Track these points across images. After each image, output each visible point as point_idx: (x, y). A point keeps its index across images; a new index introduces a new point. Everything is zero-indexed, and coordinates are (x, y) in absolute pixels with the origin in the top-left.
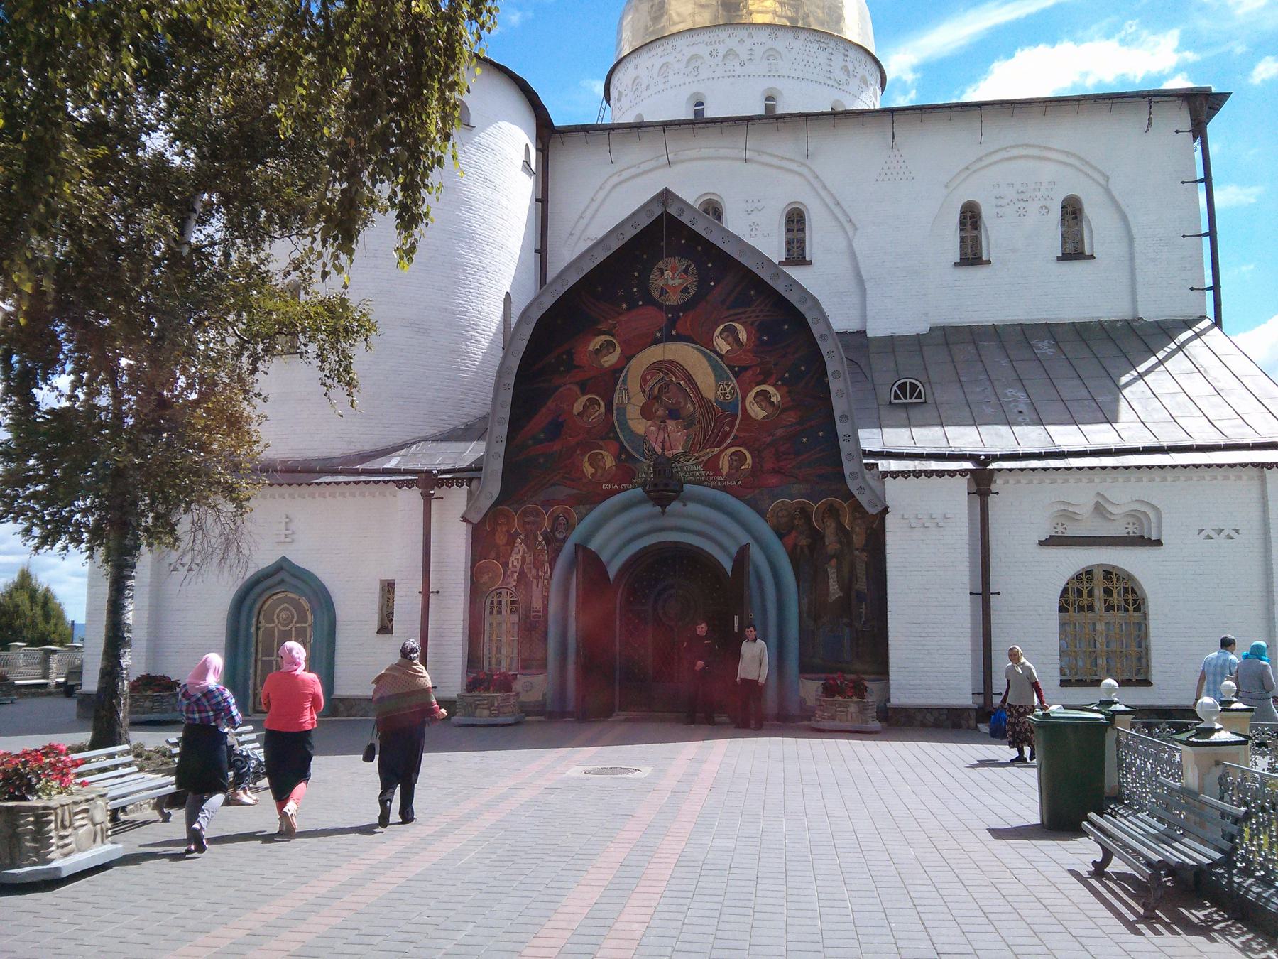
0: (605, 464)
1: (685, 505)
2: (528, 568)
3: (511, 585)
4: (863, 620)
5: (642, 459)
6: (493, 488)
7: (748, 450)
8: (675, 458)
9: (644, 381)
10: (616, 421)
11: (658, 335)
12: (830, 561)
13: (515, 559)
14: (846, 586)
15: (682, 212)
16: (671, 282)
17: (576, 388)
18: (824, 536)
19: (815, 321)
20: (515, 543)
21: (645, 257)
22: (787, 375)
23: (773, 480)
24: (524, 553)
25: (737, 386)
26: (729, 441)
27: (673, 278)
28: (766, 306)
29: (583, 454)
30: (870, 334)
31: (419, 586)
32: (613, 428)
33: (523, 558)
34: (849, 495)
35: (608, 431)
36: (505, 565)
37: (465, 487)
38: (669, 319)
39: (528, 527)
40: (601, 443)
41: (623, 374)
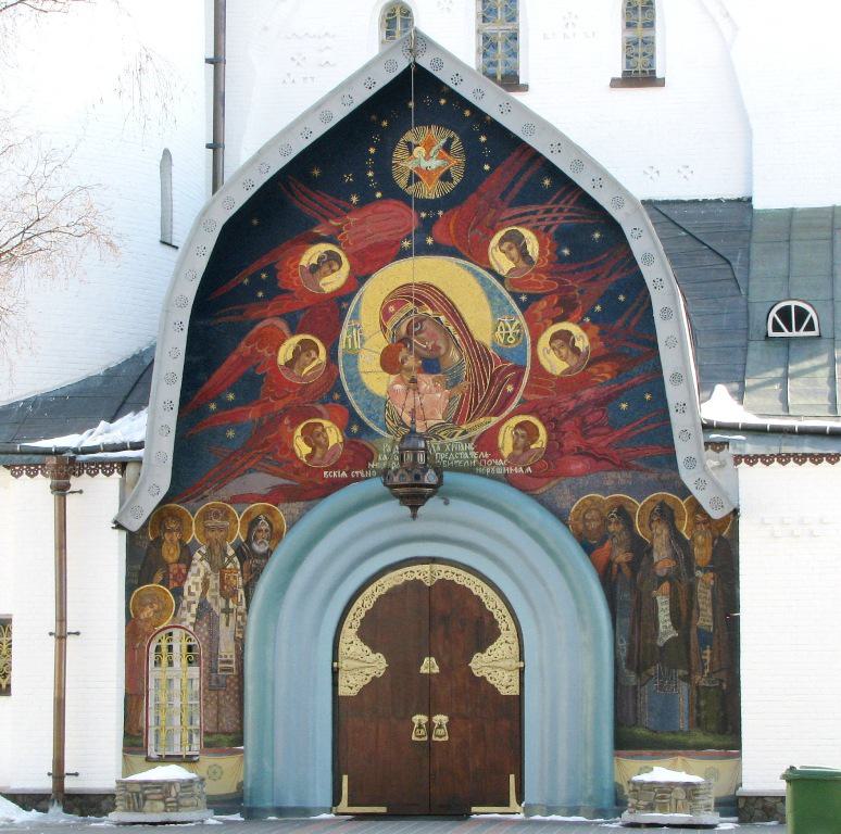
0: (327, 439)
1: (446, 503)
2: (213, 597)
3: (188, 623)
5: (382, 432)
6: (160, 478)
7: (541, 419)
8: (432, 433)
9: (386, 315)
10: (343, 376)
11: (406, 244)
13: (193, 583)
14: (681, 618)
15: (439, 64)
16: (424, 164)
17: (282, 325)
18: (652, 547)
19: (636, 233)
20: (191, 558)
21: (385, 124)
22: (598, 308)
23: (577, 466)
24: (206, 574)
25: (525, 325)
26: (513, 407)
27: (427, 158)
28: (566, 203)
29: (294, 425)
30: (757, 205)
31: (51, 624)
32: (339, 388)
33: (206, 583)
34: (684, 492)
35: (331, 392)
36: (178, 592)
37: (116, 476)
38: (421, 220)
39: (210, 534)
40: (320, 407)
41: (354, 302)
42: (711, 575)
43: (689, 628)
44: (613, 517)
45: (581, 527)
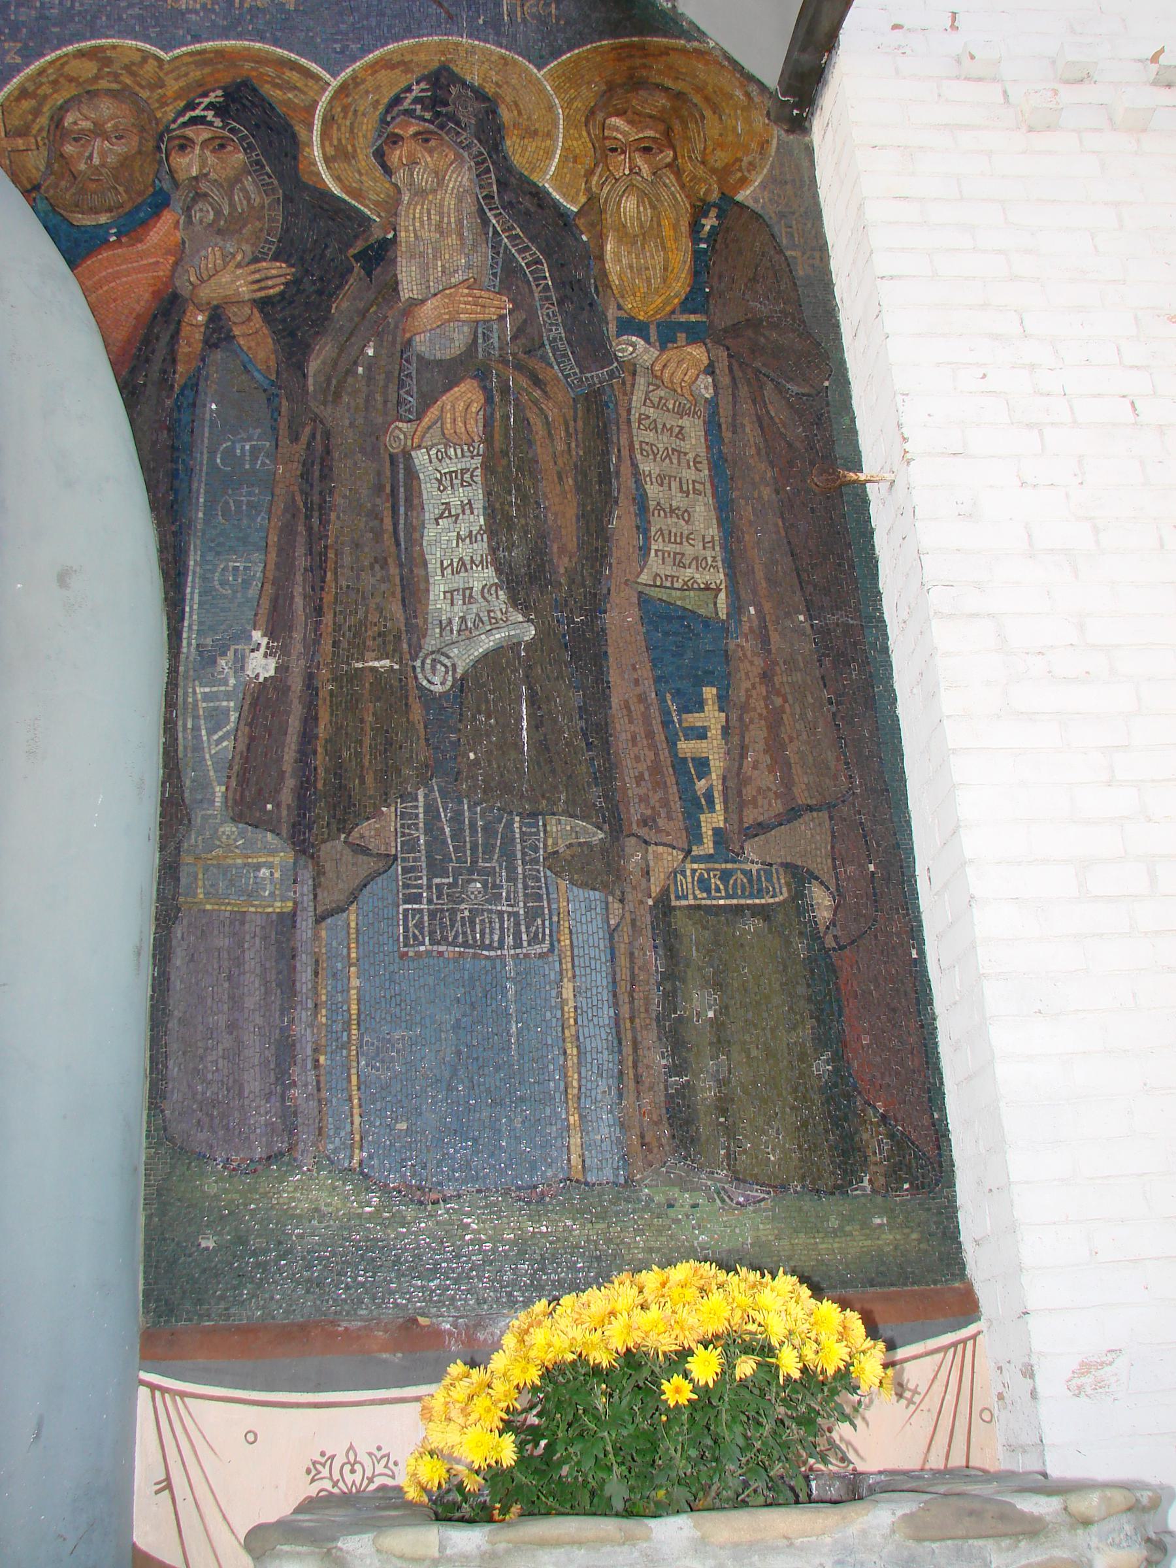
4: (712, 820)
12: (427, 402)
42: (698, 353)
43: (595, 604)
44: (194, 121)
45: (36, 162)
